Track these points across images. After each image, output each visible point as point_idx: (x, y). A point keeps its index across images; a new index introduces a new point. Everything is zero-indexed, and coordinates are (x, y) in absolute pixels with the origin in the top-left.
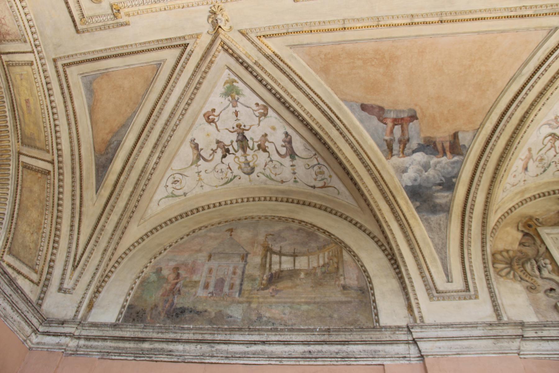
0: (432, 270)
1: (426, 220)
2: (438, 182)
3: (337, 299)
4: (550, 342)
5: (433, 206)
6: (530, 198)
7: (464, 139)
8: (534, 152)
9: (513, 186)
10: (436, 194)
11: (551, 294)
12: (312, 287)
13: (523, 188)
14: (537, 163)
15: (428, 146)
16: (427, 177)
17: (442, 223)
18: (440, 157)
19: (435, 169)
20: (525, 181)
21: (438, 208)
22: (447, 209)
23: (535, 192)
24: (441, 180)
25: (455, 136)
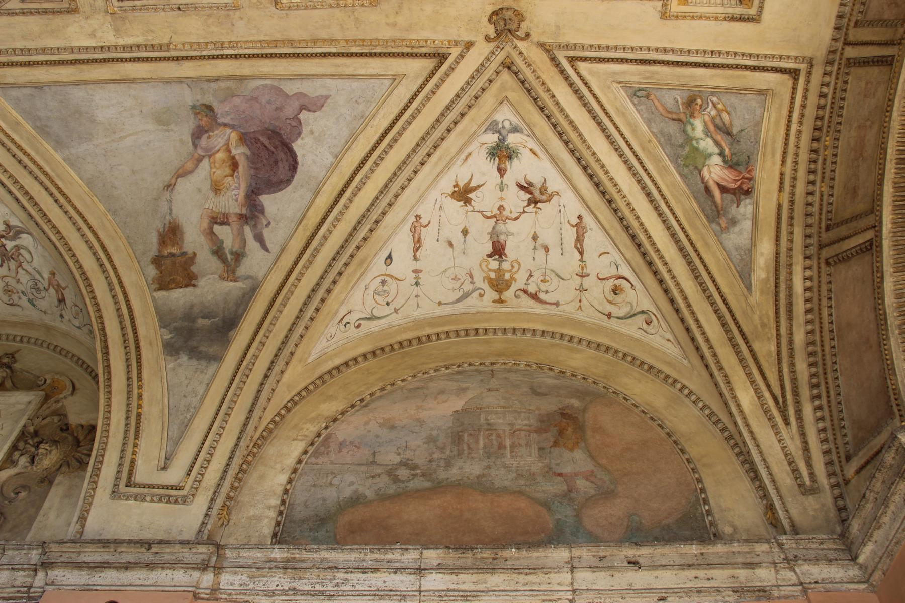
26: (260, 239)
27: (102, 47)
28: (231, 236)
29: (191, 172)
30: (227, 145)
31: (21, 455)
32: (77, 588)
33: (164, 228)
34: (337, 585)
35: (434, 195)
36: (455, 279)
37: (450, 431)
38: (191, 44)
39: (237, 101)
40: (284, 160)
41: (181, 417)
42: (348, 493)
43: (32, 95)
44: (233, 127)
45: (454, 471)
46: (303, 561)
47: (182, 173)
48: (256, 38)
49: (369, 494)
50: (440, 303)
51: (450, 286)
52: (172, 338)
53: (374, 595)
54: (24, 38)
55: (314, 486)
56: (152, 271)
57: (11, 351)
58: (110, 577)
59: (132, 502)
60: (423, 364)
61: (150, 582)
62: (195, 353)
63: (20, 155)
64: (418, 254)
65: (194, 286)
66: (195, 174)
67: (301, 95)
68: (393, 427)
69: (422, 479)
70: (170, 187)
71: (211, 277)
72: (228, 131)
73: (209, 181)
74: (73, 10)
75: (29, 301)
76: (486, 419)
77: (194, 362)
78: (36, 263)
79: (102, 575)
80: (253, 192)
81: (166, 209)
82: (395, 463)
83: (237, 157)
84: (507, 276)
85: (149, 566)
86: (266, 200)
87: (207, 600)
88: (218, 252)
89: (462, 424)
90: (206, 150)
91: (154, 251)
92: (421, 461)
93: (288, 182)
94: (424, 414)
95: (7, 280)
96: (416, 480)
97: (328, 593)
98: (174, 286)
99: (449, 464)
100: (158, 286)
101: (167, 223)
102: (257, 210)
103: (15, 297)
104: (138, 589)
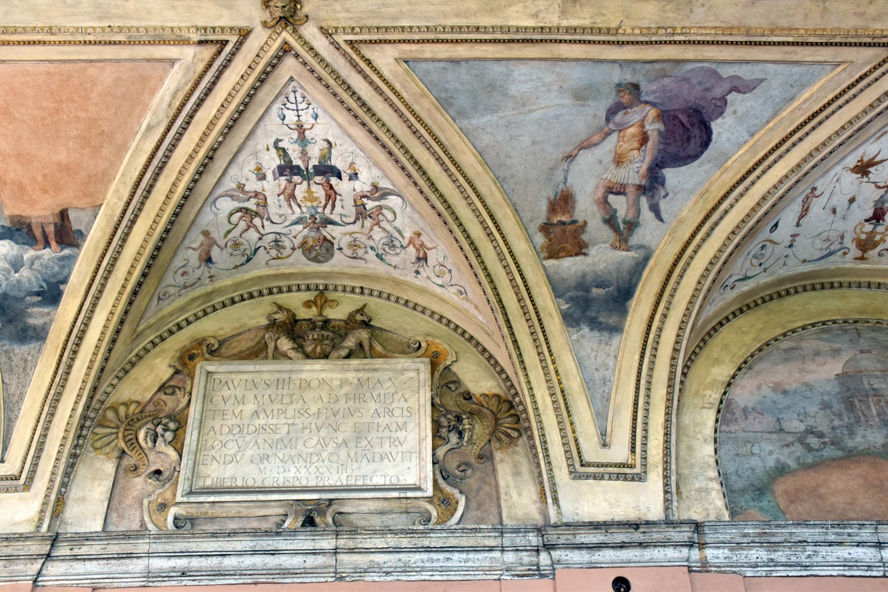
2: (36, 289)
5: (22, 329)
7: (76, 220)
8: (217, 235)
9: (185, 287)
10: (29, 310)
11: (150, 481)
13: (209, 288)
14: (230, 250)
15: (18, 230)
16: (19, 281)
17: (30, 358)
18: (40, 249)
19: (31, 268)
20: (211, 277)
21: (30, 333)
22: (39, 335)
23: (233, 292)
24: (41, 287)
25: (63, 215)
26: (655, 210)
27: (542, 28)
29: (596, 145)
30: (643, 121)
31: (449, 431)
32: (584, 566)
34: (809, 556)
35: (838, 168)
36: (827, 240)
37: (839, 396)
38: (641, 29)
39: (666, 81)
40: (698, 137)
41: (600, 391)
42: (771, 462)
43: (445, 68)
44: (654, 105)
45: (859, 439)
46: (773, 535)
47: (586, 145)
48: (711, 24)
49: (792, 463)
50: (804, 261)
51: (819, 246)
52: (568, 308)
53: (844, 566)
54: (457, 15)
55: (738, 455)
56: (540, 239)
57: (358, 306)
58: (608, 555)
59: (591, 481)
60: (790, 322)
62: (595, 324)
63: (418, 126)
64: (801, 221)
65: (585, 254)
66: (599, 147)
67: (737, 77)
68: (785, 392)
69: (832, 447)
70: (570, 158)
71: (603, 245)
72: (648, 108)
73: (613, 154)
75: (377, 255)
76: (869, 384)
77: (596, 334)
78: (397, 223)
79: (601, 553)
80: (657, 165)
81: (559, 176)
82: (802, 430)
83: (649, 133)
84: (878, 238)
85: (641, 545)
86: (670, 174)
87: (699, 571)
88: (610, 221)
89: (849, 389)
92: (824, 427)
93: (696, 157)
94: (809, 378)
96: (827, 449)
97: (804, 564)
99: (852, 434)
100: (547, 254)
101: (559, 191)
102: (656, 181)
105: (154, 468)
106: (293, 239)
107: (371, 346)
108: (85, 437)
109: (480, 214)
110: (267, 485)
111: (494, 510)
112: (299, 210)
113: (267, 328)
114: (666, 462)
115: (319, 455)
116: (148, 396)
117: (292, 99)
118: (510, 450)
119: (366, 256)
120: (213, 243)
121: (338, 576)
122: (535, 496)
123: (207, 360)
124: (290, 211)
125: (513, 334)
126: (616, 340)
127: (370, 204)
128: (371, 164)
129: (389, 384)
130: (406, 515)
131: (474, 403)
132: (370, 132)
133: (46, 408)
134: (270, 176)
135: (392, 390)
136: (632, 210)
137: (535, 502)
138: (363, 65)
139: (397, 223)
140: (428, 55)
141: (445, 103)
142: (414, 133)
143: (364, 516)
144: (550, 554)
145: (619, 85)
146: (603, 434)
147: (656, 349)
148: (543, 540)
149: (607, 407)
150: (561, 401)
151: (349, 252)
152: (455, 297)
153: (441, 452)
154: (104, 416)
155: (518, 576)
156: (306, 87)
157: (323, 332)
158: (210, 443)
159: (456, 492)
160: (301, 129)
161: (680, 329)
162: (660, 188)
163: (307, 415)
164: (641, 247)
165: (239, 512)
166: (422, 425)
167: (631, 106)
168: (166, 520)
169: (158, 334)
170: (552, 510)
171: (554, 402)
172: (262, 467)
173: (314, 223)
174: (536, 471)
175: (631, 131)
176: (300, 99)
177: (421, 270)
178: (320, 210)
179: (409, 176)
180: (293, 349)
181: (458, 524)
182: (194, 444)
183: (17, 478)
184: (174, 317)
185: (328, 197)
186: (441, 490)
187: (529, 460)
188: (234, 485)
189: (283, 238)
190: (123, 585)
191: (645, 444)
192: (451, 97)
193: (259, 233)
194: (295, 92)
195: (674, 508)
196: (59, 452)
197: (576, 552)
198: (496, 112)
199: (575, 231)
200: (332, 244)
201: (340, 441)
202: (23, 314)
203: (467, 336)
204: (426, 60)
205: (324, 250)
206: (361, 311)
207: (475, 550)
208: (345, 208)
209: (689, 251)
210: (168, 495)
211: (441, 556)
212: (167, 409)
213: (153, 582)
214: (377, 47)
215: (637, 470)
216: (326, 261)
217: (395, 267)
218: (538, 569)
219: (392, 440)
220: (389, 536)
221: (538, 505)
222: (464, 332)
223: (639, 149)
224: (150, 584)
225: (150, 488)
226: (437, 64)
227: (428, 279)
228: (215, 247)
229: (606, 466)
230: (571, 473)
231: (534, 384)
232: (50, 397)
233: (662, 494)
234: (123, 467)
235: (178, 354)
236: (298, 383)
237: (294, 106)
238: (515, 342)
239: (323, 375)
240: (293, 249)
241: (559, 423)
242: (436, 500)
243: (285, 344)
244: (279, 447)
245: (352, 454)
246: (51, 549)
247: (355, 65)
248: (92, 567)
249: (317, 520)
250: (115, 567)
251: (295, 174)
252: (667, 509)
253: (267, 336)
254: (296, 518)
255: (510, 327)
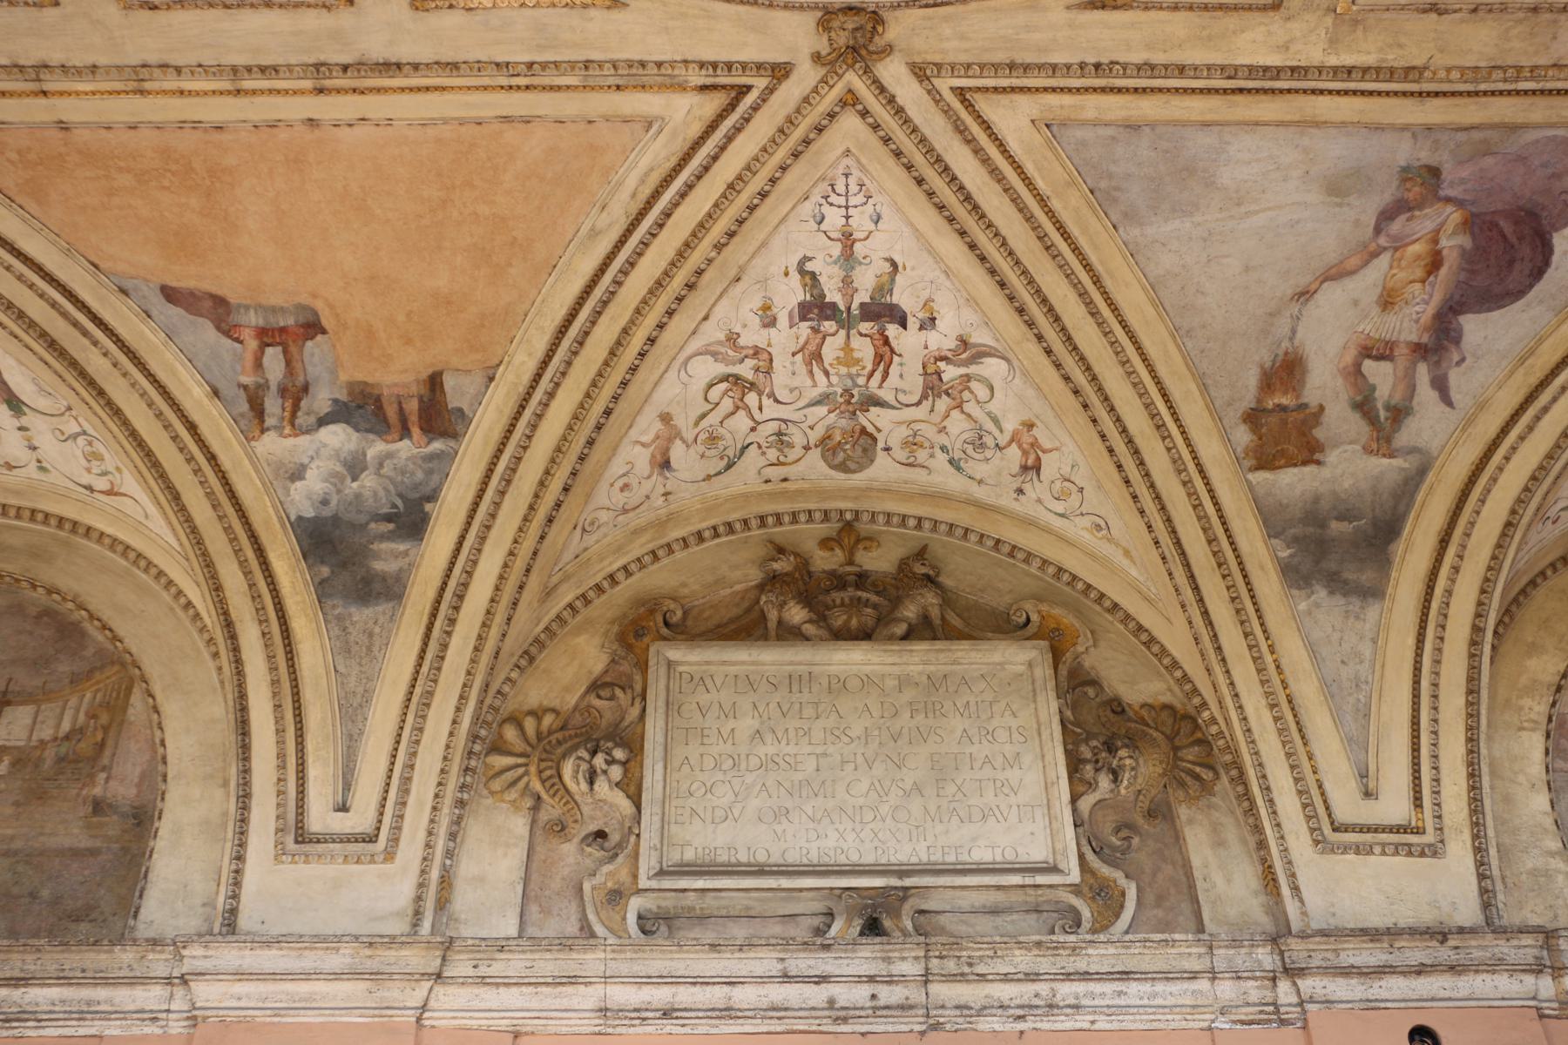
0: (313, 772)
1: (339, 618)
3: (67, 842)
4: (502, 990)
6: (684, 540)
8: (683, 422)
9: (625, 511)
11: (589, 849)
12: (17, 804)
14: (701, 448)
17: (377, 630)
20: (666, 494)
21: (377, 586)
26: (1441, 385)
28: (1391, 379)
30: (1437, 231)
31: (1097, 770)
33: (1274, 361)
41: (1351, 700)
43: (1113, 138)
52: (1291, 556)
57: (914, 546)
58: (1394, 987)
59: (1351, 857)
61: (1463, 993)
62: (1337, 584)
65: (1318, 463)
66: (1358, 277)
70: (1304, 295)
71: (1349, 447)
72: (1450, 209)
74: (1276, 7)
75: (951, 462)
77: (1339, 600)
78: (993, 407)
79: (1382, 983)
80: (1451, 308)
81: (1286, 330)
83: (1445, 252)
86: (1473, 326)
88: (1364, 406)
90: (1395, 238)
91: (1248, 400)
93: (1520, 293)
95: (916, 426)
98: (1282, 462)
100: (1254, 462)
101: (1281, 353)
103: (922, 455)
104: (1451, 1004)
105: (593, 827)
106: (808, 431)
107: (943, 618)
108: (474, 771)
109: (1147, 392)
110: (790, 861)
111: (1186, 907)
112: (824, 379)
113: (761, 587)
114: (1477, 824)
115: (875, 809)
116: (572, 700)
117: (840, 188)
118: (1203, 802)
119: (931, 463)
120: (675, 434)
121: (931, 1021)
122: (1255, 883)
123: (665, 639)
124: (809, 382)
125: (1201, 600)
126: (1373, 612)
127: (950, 373)
128: (962, 301)
129: (983, 685)
130: (1035, 916)
131: (1130, 720)
132: (972, 246)
133: (410, 718)
134: (783, 320)
135: (988, 696)
136: (1401, 387)
137: (1256, 893)
138: (976, 129)
139: (993, 407)
140: (1090, 114)
141: (1102, 198)
142: (1047, 248)
143: (964, 917)
144: (1295, 984)
145: (1405, 169)
146: (1363, 775)
147: (1443, 627)
148: (1283, 960)
149: (1366, 728)
150: (1290, 717)
151: (901, 455)
152: (1087, 536)
153: (1086, 804)
154: (501, 736)
155: (1243, 1022)
156: (870, 168)
157: (859, 593)
158: (684, 786)
159: (1118, 875)
160: (848, 240)
161: (1483, 591)
162: (1453, 348)
163: (846, 740)
164: (1413, 450)
165: (748, 908)
166: (1049, 758)
167: (1420, 206)
168: (624, 919)
169: (579, 592)
170: (1291, 907)
171: (1276, 719)
172: (779, 829)
173: (849, 403)
174: (1252, 841)
175: (1417, 248)
176: (854, 188)
177: (1027, 487)
178: (861, 381)
179: (1031, 324)
180: (810, 621)
181: (1127, 932)
182: (659, 787)
183: (372, 839)
184: (606, 563)
185: (879, 358)
186: (1093, 873)
187: (1237, 819)
188: (733, 860)
189: (792, 429)
190: (564, 1030)
191: (1438, 793)
192: (1117, 189)
193: (753, 419)
194: (847, 176)
195: (1501, 906)
196: (437, 796)
197: (1341, 981)
198: (1191, 214)
199: (1304, 422)
200: (875, 440)
201: (908, 785)
202: (361, 555)
203: (1107, 604)
204: (1084, 123)
205: (859, 450)
206: (921, 554)
207: (1167, 976)
208: (906, 377)
209: (1497, 458)
210: (624, 875)
211: (1109, 987)
212: (604, 723)
213: (615, 1027)
214: (1004, 99)
215: (1429, 838)
216: (861, 468)
217: (980, 482)
218: (1277, 1012)
219: (999, 784)
220: (1017, 952)
221: (1263, 898)
222: (1102, 595)
223: (1423, 282)
224: (610, 1030)
225: (588, 862)
226: (1102, 131)
227: (1039, 502)
228: (678, 442)
229: (1376, 831)
230: (1317, 842)
231: (1241, 687)
232: (415, 699)
233: (1474, 880)
234: (541, 824)
235: (616, 629)
236: (825, 682)
237: (842, 201)
238: (1205, 613)
239: (868, 669)
240: (807, 448)
241: (1288, 755)
242: (1086, 890)
243: (796, 614)
244: (804, 794)
245: (932, 808)
246: (442, 965)
247: (961, 130)
248: (511, 997)
249: (887, 923)
250: (548, 998)
251: (827, 319)
252: (1486, 906)
253: (764, 598)
254: (849, 921)
255: (1196, 589)
